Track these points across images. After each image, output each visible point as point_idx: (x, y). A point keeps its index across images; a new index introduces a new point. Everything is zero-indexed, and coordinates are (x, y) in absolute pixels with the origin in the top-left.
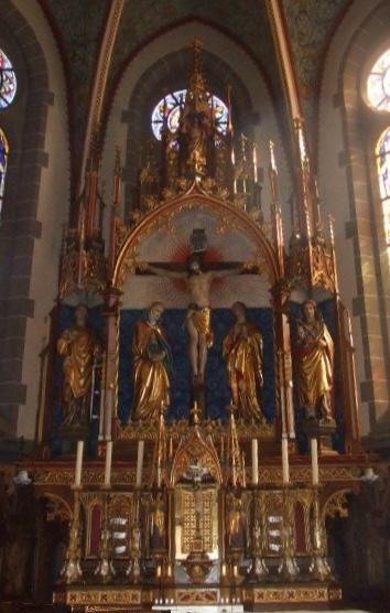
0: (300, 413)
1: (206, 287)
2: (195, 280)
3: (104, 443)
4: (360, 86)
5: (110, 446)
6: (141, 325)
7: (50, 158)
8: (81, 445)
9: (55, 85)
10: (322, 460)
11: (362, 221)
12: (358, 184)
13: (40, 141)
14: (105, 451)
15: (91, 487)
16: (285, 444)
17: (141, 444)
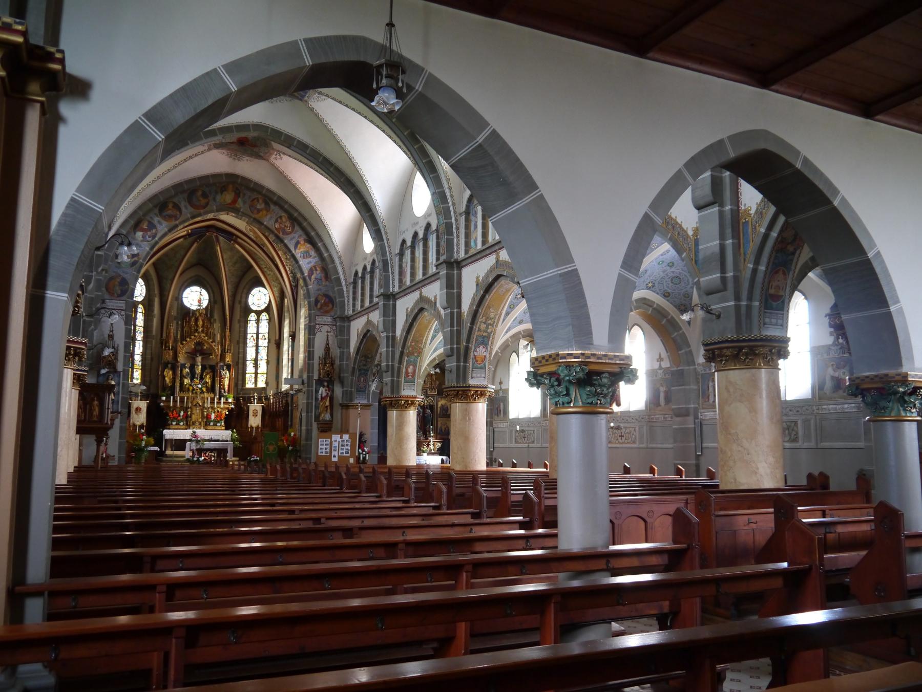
0: (220, 392)
1: (200, 360)
2: (198, 358)
3: (177, 397)
4: (247, 298)
5: (178, 398)
6: (184, 369)
7: (156, 317)
8: (172, 397)
9: (157, 291)
10: (224, 403)
11: (241, 340)
12: (242, 329)
13: (153, 311)
14: (177, 398)
15: (175, 406)
16: (216, 398)
17: (186, 397)
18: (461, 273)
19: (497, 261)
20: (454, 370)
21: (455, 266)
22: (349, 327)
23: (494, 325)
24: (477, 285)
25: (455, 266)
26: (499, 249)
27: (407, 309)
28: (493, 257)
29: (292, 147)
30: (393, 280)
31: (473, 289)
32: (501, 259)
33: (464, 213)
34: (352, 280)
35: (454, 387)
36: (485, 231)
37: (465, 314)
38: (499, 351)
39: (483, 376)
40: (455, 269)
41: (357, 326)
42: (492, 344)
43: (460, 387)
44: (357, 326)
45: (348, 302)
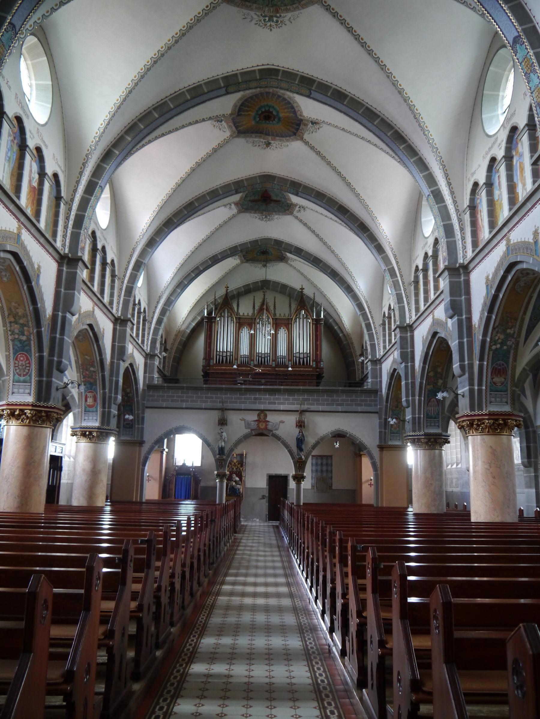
18: (469, 278)
19: (507, 248)
20: (467, 394)
21: (461, 271)
22: (381, 369)
23: (516, 335)
24: (487, 286)
25: (461, 271)
26: (509, 232)
27: (423, 337)
28: (504, 242)
29: (300, 194)
30: (410, 310)
31: (484, 292)
32: (512, 242)
33: (468, 209)
34: (381, 322)
35: (467, 416)
36: (493, 219)
37: (477, 326)
38: (528, 368)
39: (504, 400)
40: (462, 275)
41: (386, 367)
42: (515, 360)
43: (475, 415)
44: (386, 367)
45: (379, 344)
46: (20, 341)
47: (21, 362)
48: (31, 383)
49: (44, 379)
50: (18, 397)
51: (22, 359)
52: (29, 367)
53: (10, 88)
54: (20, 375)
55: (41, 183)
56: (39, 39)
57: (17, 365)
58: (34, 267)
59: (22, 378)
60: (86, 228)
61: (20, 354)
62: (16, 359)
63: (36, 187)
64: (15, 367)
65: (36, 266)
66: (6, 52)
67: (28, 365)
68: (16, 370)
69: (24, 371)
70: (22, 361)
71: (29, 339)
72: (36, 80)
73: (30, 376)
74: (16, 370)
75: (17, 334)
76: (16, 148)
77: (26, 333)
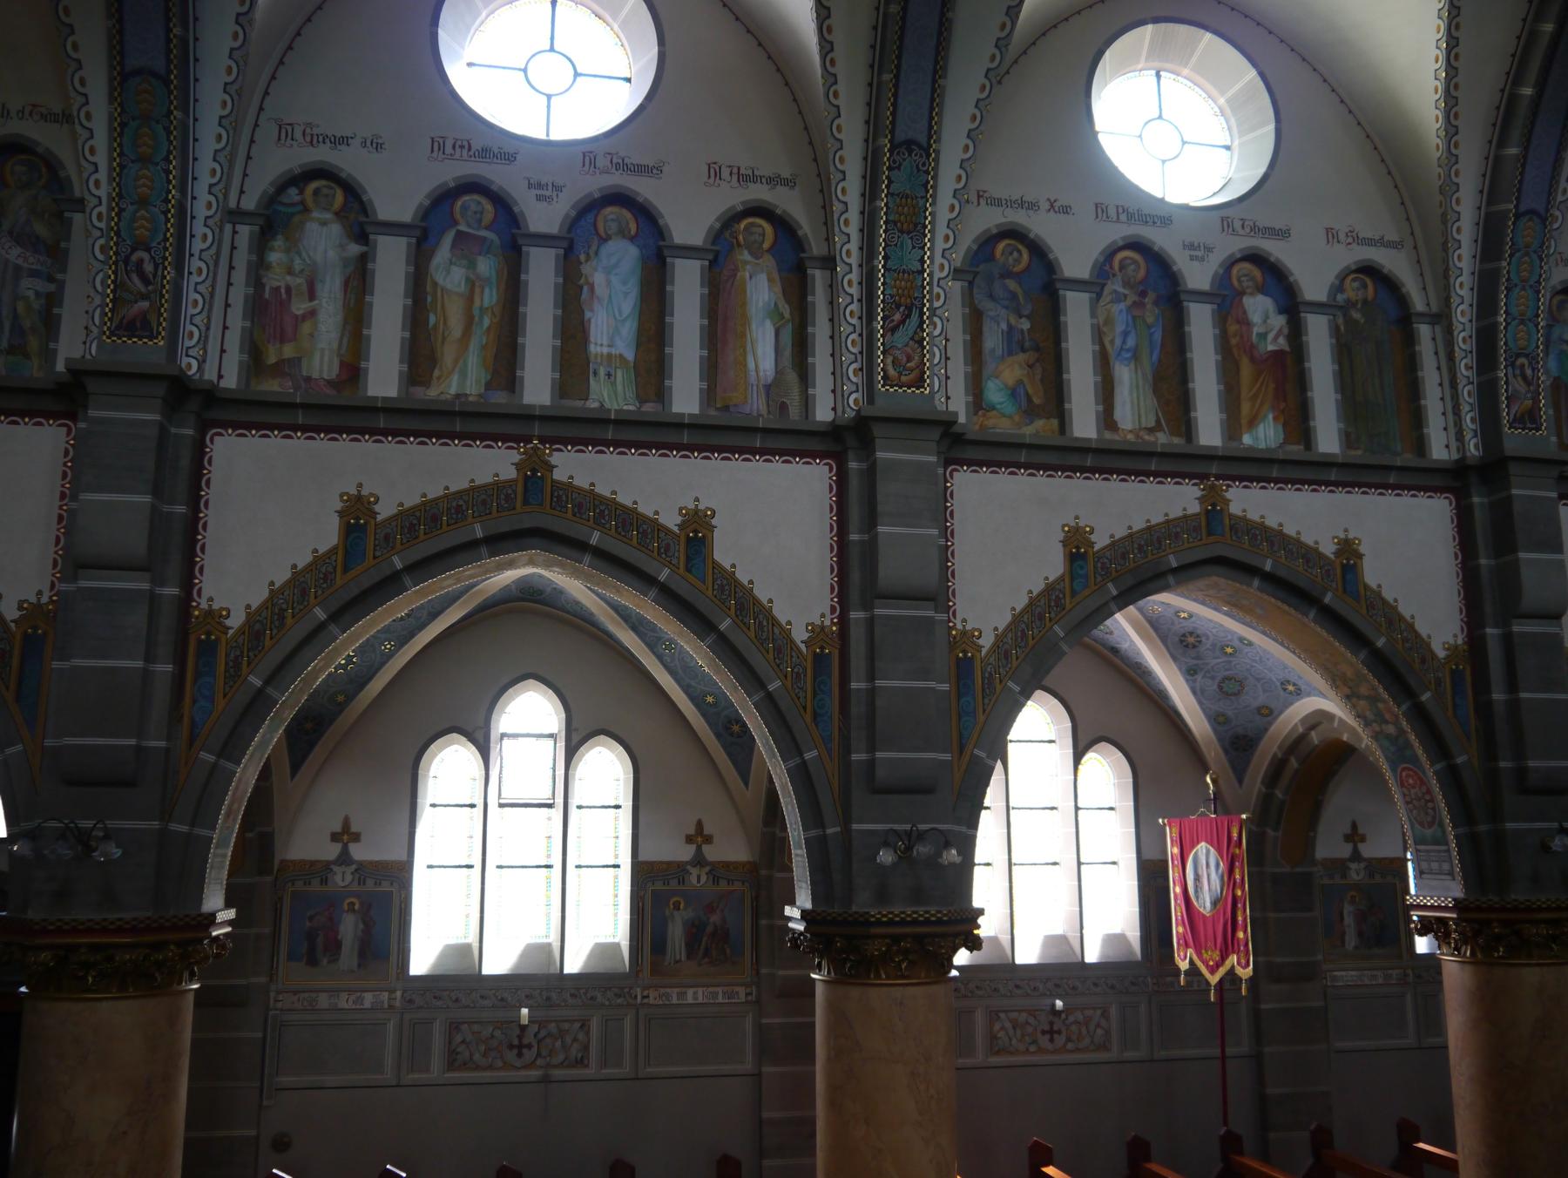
46: (1388, 736)
47: (1413, 791)
48: (1447, 844)
49: (1483, 828)
50: (1434, 883)
51: (1411, 781)
52: (1432, 800)
53: (1066, 210)
54: (1421, 824)
55: (1296, 331)
56: (1156, 20)
57: (1408, 799)
58: (1321, 556)
59: (1429, 832)
60: (1518, 355)
61: (1404, 769)
62: (1402, 785)
63: (1287, 348)
64: (1407, 803)
65: (1328, 549)
66: (921, 202)
67: (1428, 797)
68: (1411, 811)
69: (1427, 814)
70: (1414, 787)
71: (1402, 732)
72: (1222, 93)
73: (1441, 825)
74: (1411, 811)
75: (1375, 721)
76: (1151, 314)
77: (1387, 716)
